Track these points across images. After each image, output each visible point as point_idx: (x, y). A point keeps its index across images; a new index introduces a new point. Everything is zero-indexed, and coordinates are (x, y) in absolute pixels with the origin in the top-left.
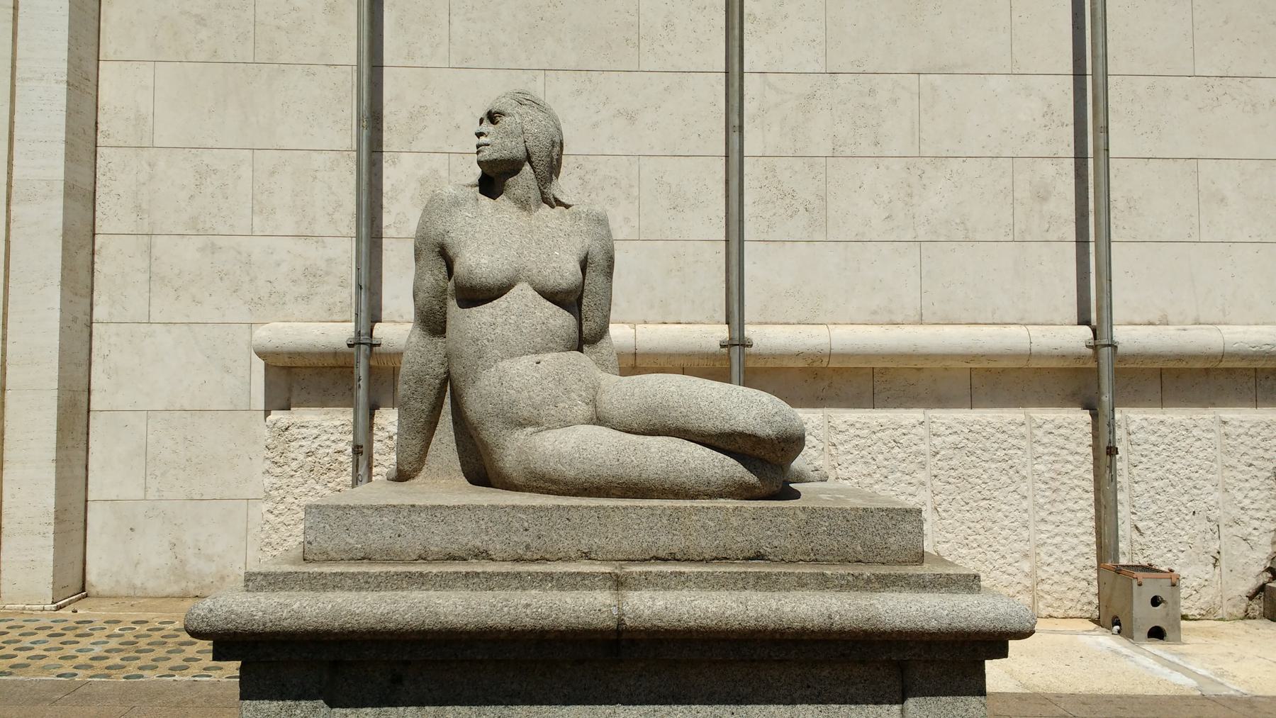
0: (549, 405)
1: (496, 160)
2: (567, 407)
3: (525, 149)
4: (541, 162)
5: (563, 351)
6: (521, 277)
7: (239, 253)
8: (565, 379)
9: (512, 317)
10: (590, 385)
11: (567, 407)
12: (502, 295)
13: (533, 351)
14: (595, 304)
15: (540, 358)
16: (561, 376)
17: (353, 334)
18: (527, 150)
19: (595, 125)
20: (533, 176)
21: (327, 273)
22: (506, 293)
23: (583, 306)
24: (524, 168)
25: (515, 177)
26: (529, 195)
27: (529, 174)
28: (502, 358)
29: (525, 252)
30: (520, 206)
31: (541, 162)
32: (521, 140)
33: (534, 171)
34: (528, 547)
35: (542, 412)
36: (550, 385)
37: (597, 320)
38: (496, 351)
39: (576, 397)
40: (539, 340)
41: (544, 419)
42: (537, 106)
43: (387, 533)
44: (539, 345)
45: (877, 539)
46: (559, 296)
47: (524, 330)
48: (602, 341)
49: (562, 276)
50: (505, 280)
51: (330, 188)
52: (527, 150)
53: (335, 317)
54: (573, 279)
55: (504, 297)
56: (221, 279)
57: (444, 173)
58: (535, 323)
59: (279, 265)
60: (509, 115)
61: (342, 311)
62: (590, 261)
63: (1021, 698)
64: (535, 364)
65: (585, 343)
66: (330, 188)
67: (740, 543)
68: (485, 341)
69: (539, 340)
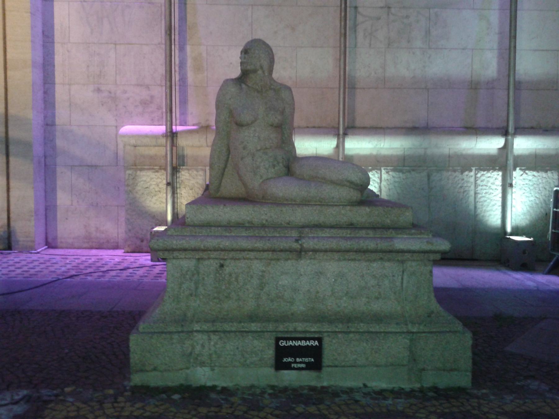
7: (110, 92)
17: (165, 132)
19: (276, 32)
21: (151, 102)
34: (267, 221)
43: (216, 215)
45: (396, 218)
51: (151, 62)
53: (155, 123)
56: (102, 105)
57: (204, 55)
59: (128, 99)
61: (158, 120)
63: (460, 290)
66: (151, 62)
67: (344, 220)
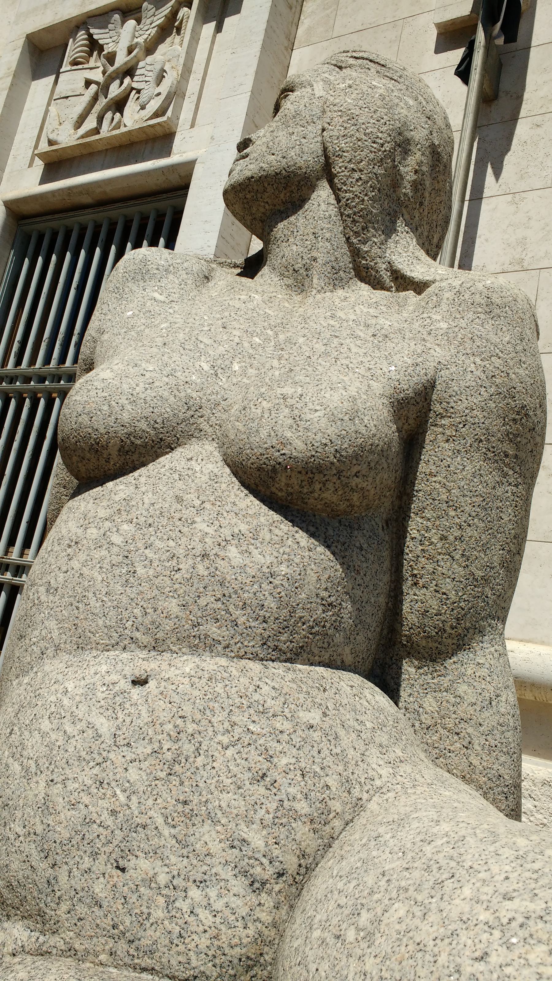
0: (95, 855)
1: (249, 179)
2: (163, 879)
3: (320, 152)
4: (356, 175)
5: (255, 657)
6: (204, 426)
8: (200, 761)
9: (125, 527)
10: (303, 807)
11: (163, 879)
12: (135, 469)
13: (145, 639)
14: (443, 538)
15: (153, 665)
16: (188, 748)
18: (325, 149)
20: (333, 211)
22: (144, 465)
23: (409, 542)
24: (314, 196)
25: (292, 219)
26: (315, 254)
27: (323, 207)
28: (57, 648)
29: (236, 367)
30: (290, 282)
31: (356, 175)
32: (313, 130)
33: (338, 200)
35: (63, 878)
36: (133, 774)
37: (447, 586)
38: (52, 624)
39: (215, 847)
40: (173, 606)
41: (64, 907)
42: (379, 68)
44: (168, 625)
46: (282, 479)
47: (140, 571)
48: (461, 656)
49: (297, 419)
50: (143, 425)
52: (325, 149)
54: (332, 431)
55: (136, 474)
58: (181, 552)
60: (302, 85)
62: (437, 408)
64: (124, 685)
65: (409, 655)
68: (42, 589)
69: (173, 606)
